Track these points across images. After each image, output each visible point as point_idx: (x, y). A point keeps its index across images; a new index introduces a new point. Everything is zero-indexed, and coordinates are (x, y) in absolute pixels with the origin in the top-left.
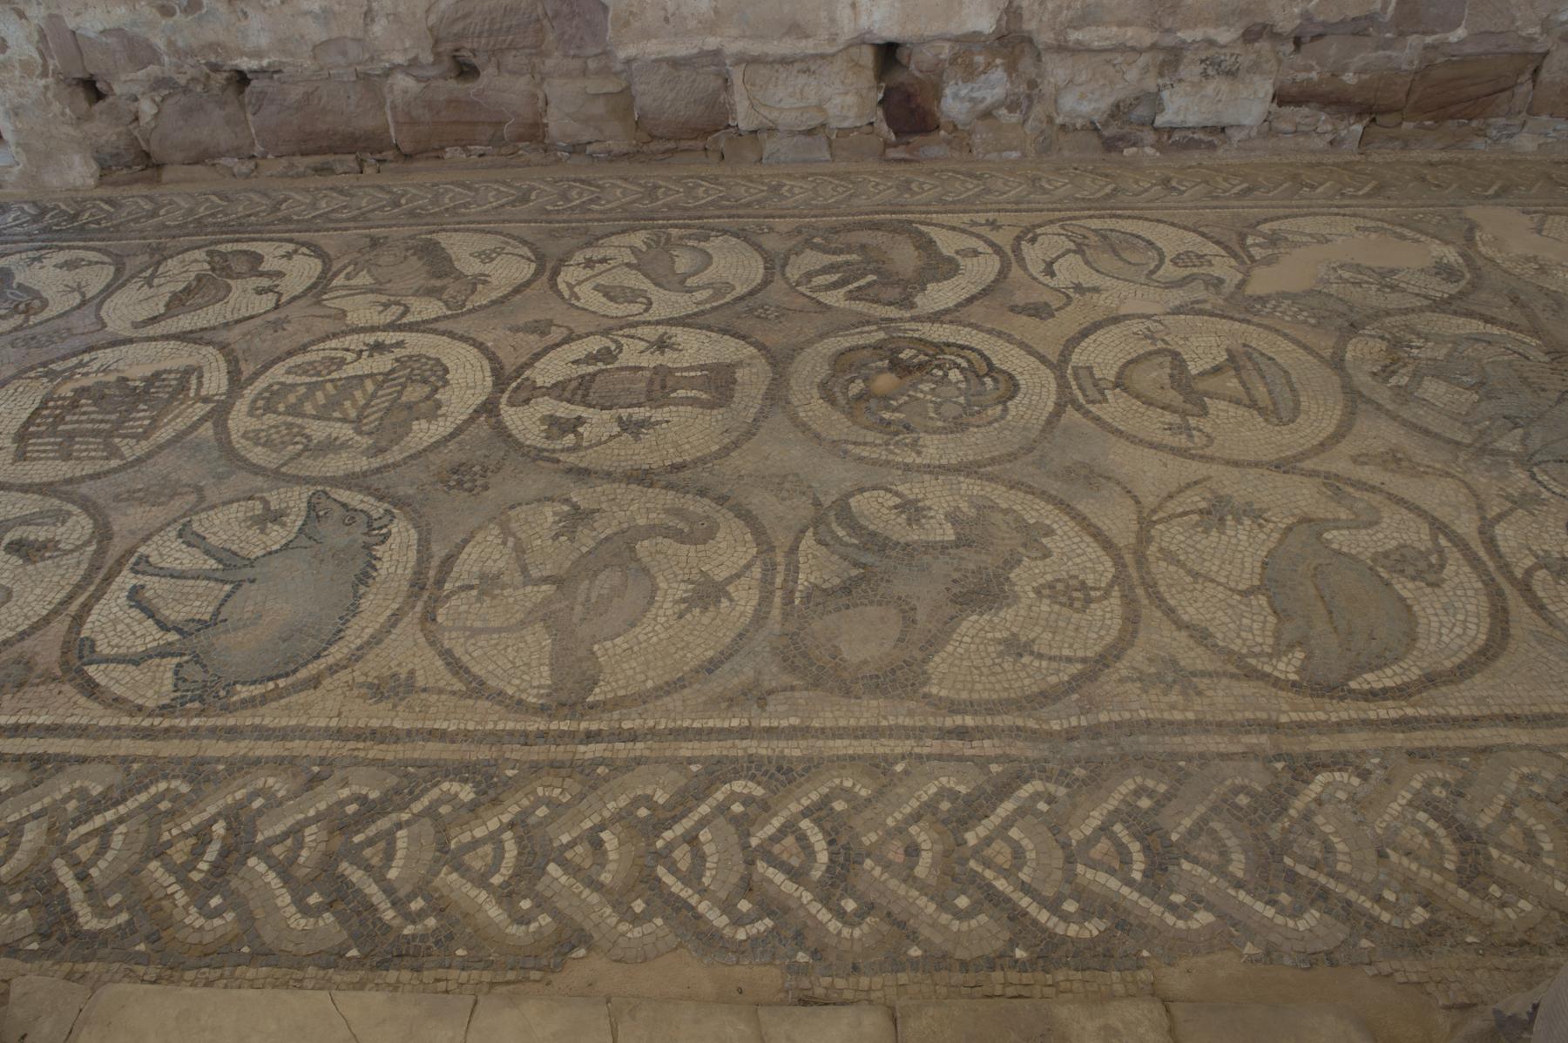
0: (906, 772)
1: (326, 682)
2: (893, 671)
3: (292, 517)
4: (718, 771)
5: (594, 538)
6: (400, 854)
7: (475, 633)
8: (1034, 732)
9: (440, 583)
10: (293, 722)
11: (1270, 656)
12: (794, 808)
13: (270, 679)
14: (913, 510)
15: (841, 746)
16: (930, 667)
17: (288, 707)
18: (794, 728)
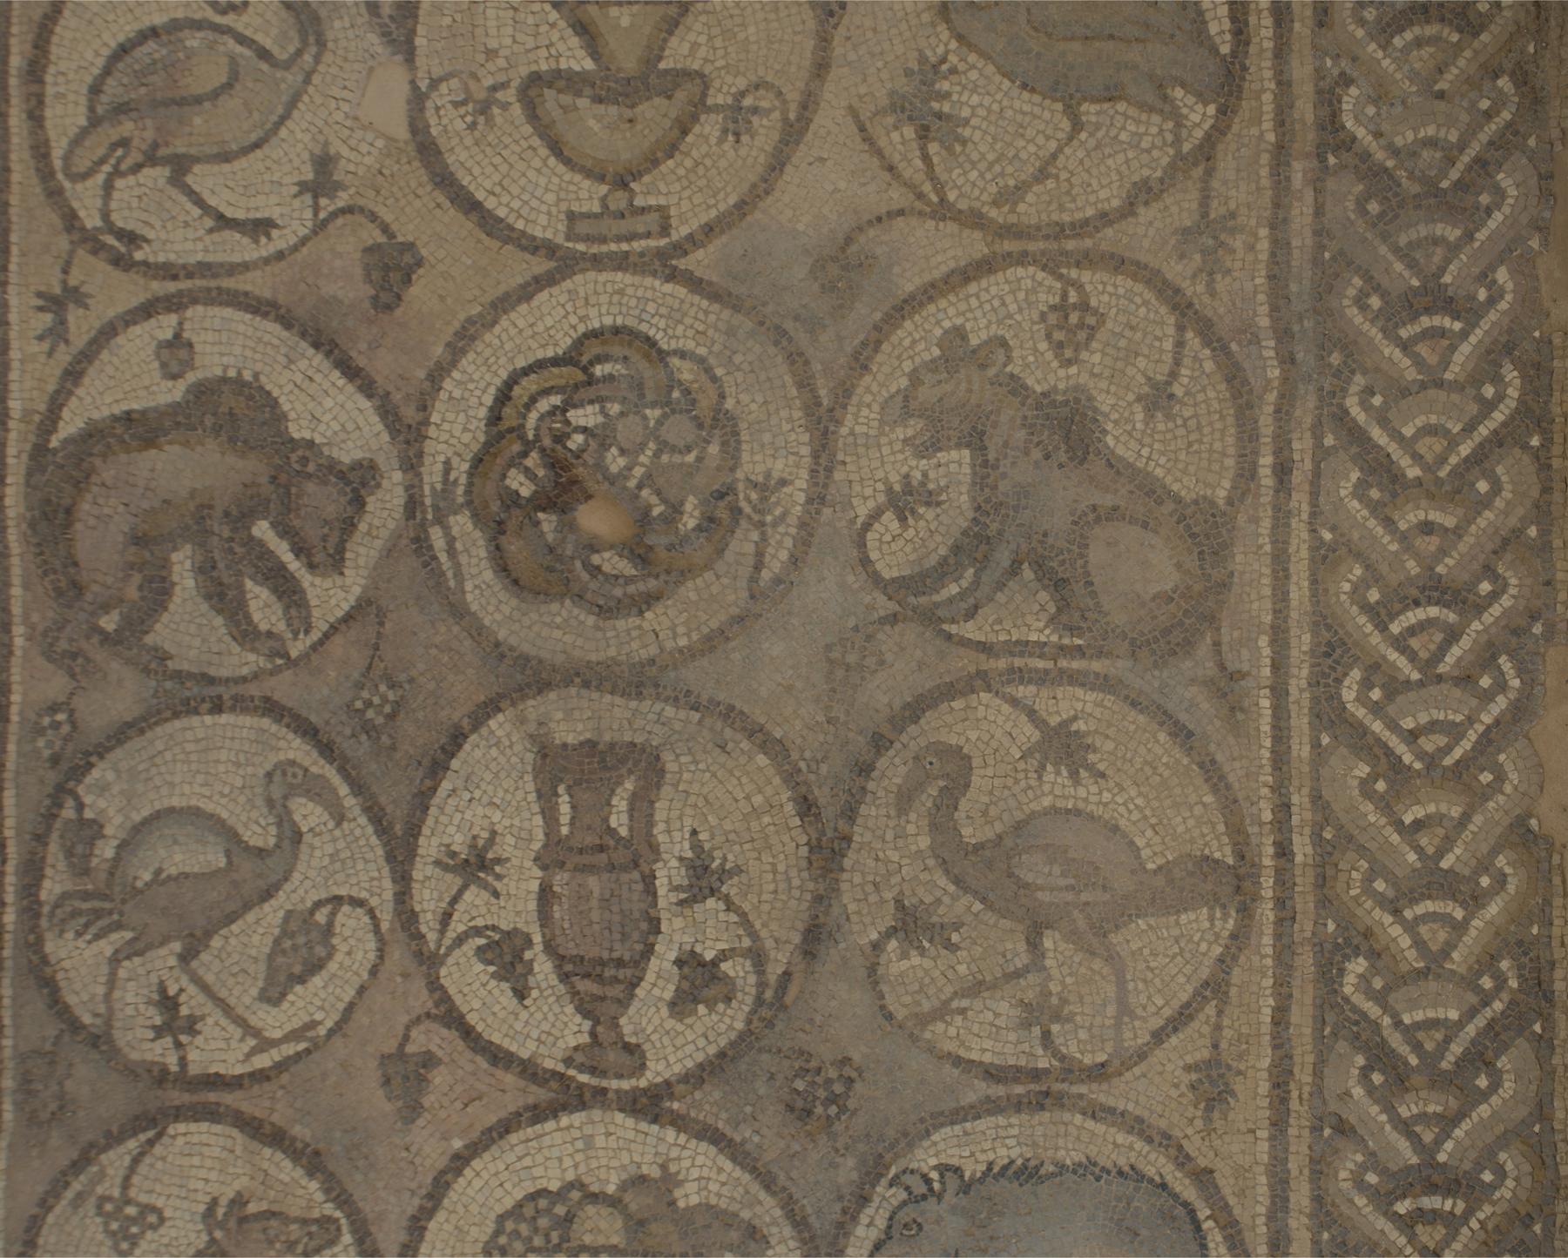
0: (1333, 529)
1: (1202, 1162)
2: (1193, 536)
4: (1329, 714)
5: (954, 898)
6: (1431, 1014)
7: (1125, 1009)
8: (1282, 396)
11: (1179, 125)
12: (1376, 639)
13: (1198, 1228)
14: (905, 501)
15: (1299, 591)
16: (1188, 496)
18: (1273, 642)
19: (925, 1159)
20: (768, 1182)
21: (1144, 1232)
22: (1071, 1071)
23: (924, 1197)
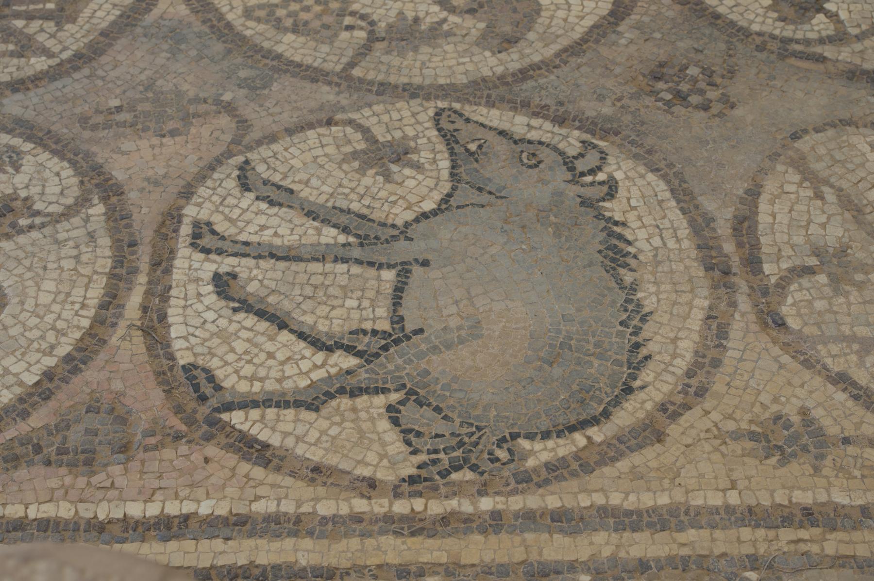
1: (673, 430)
9: (753, 263)
10: (664, 500)
13: (572, 429)
21: (557, 371)
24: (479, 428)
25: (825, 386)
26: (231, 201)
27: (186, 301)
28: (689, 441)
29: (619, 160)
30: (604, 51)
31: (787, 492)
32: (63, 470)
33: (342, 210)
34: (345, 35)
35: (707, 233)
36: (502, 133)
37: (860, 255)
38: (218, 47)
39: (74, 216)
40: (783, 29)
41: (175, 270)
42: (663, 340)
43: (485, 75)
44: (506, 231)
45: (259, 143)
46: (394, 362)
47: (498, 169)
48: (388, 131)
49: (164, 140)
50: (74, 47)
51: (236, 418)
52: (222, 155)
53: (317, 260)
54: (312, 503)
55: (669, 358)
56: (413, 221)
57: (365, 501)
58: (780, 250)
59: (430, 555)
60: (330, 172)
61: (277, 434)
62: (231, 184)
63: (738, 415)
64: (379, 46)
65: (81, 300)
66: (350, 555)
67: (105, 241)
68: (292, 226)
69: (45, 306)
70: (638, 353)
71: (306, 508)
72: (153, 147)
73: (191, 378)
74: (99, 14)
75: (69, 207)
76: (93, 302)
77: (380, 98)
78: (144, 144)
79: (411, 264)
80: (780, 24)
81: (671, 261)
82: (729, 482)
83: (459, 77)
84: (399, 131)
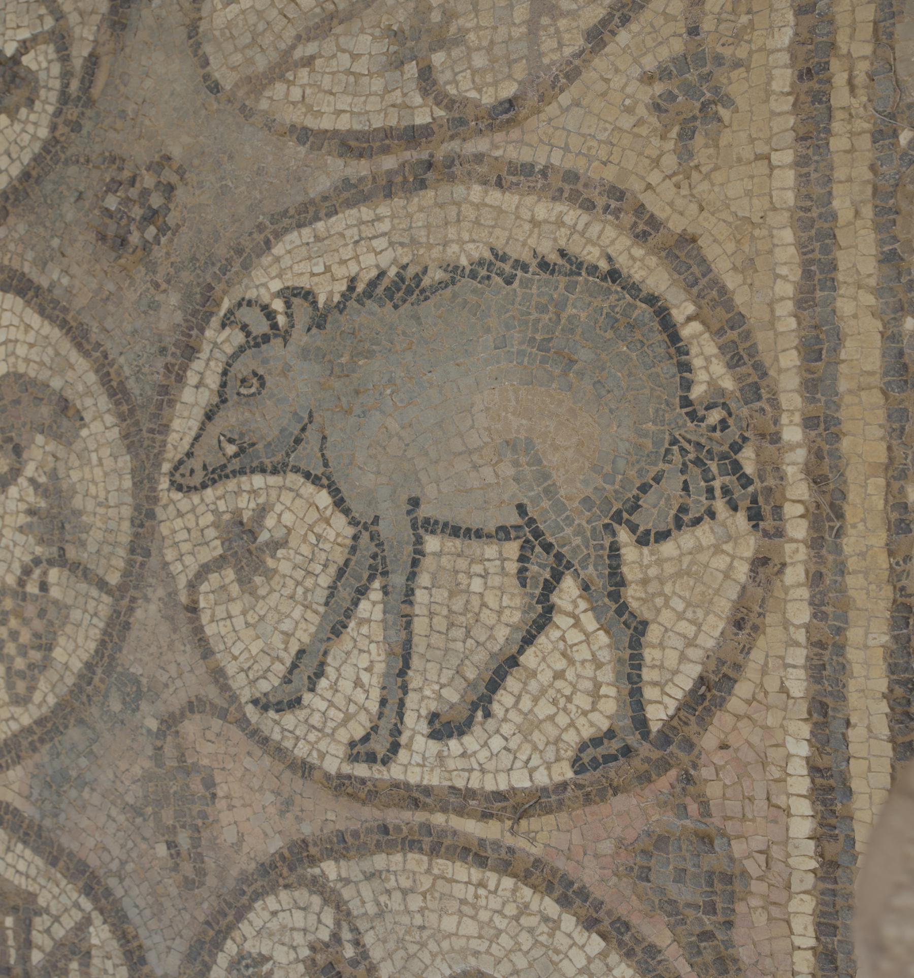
1: (677, 224)
3: (242, 504)
9: (413, 136)
13: (674, 338)
17: (748, 266)
19: (266, 283)
20: (79, 337)
21: (584, 355)
22: (462, 122)
23: (266, 339)
24: (674, 441)
25: (606, 55)
26: (316, 720)
27: (472, 770)
28: (694, 207)
29: (251, 285)
30: (79, 302)
31: (773, 98)
32: (740, 907)
33: (331, 595)
34: (55, 593)
35: (368, 187)
36: (209, 416)
37: (401, 15)
38: (74, 734)
39: (340, 895)
40: (46, 102)
41: (425, 782)
42: (535, 236)
43: (118, 436)
44: (363, 412)
45: (225, 688)
46: (570, 537)
47: (267, 421)
48: (207, 544)
49: (220, 794)
50: (75, 895)
51: (656, 715)
52: (243, 730)
53: (409, 624)
54: (792, 629)
55: (563, 230)
56: (347, 516)
57: (789, 570)
58: (393, 106)
59: (874, 498)
60: (270, 608)
61: (682, 668)
62: (289, 719)
63: (654, 153)
64: (72, 553)
65: (471, 889)
66: (873, 587)
67: (379, 861)
68: (356, 652)
69: (481, 928)
70: (555, 264)
71: (801, 636)
72: (231, 808)
73: (595, 764)
74: (22, 866)
75: (326, 902)
76: (476, 874)
77: (154, 552)
78: (226, 817)
79: (416, 518)
80: (38, 105)
81: (411, 227)
82: (759, 163)
83: (120, 464)
84: (206, 532)
